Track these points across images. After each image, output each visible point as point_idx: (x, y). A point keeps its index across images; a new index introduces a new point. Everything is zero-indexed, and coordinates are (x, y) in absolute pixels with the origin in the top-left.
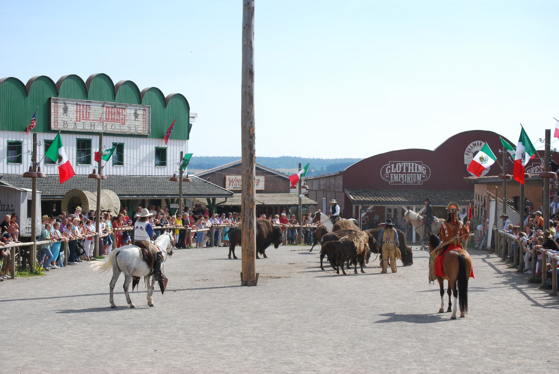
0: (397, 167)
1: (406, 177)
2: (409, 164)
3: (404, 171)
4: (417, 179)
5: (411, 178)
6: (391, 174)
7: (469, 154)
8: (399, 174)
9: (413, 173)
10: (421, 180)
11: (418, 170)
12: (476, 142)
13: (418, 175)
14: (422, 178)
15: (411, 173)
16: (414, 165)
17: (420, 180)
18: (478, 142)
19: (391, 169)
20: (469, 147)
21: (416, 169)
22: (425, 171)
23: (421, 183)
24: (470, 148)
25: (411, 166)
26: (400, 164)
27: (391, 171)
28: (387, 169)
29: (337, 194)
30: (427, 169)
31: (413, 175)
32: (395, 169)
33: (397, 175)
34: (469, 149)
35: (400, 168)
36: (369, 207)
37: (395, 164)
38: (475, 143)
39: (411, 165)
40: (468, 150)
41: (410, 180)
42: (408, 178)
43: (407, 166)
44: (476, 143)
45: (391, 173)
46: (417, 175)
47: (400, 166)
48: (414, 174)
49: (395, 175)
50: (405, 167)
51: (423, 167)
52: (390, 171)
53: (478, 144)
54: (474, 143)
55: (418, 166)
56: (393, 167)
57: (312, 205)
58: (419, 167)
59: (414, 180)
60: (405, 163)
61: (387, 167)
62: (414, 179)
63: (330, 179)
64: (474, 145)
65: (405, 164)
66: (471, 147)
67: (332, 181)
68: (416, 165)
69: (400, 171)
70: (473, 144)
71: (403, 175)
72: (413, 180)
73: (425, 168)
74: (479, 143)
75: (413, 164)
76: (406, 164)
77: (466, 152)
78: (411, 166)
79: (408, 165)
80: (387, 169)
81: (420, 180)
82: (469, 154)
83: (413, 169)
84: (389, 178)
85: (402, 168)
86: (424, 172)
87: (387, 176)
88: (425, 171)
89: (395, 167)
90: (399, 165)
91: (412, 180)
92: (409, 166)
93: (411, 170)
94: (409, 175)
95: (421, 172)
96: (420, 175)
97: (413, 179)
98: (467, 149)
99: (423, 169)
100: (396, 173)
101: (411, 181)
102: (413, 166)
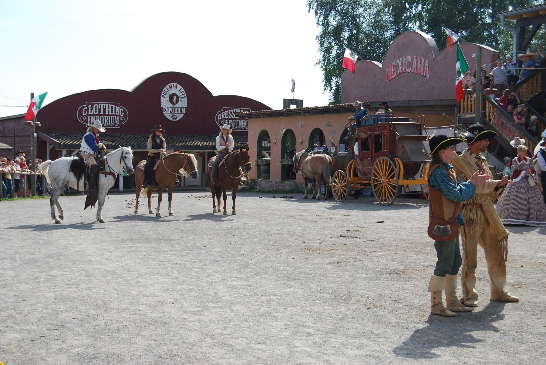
0: (94, 109)
1: (103, 119)
2: (107, 105)
3: (102, 113)
4: (114, 122)
5: (108, 121)
6: (88, 116)
7: (165, 96)
8: (97, 117)
9: (110, 115)
10: (119, 123)
11: (115, 112)
12: (172, 84)
13: (116, 117)
14: (120, 121)
15: (108, 115)
16: (112, 107)
17: (118, 123)
18: (174, 85)
19: (88, 110)
20: (165, 89)
21: (114, 111)
22: (123, 114)
23: (119, 126)
24: (166, 90)
25: (109, 108)
26: (97, 105)
27: (88, 112)
28: (84, 110)
29: (16, 140)
30: (125, 112)
31: (111, 117)
32: (92, 110)
33: (94, 117)
34: (166, 91)
35: (97, 109)
36: (73, 151)
37: (93, 105)
38: (171, 85)
39: (109, 106)
40: (165, 92)
41: (107, 123)
42: (106, 121)
43: (104, 108)
44: (172, 85)
45: (88, 115)
46: (114, 118)
47: (97, 107)
48: (112, 117)
49: (92, 117)
50: (102, 109)
51: (121, 109)
52: (87, 112)
53: (174, 87)
54: (170, 85)
55: (115, 108)
56: (90, 109)
57: (7, 151)
58: (117, 109)
59: (112, 123)
60: (103, 105)
61: (84, 109)
62: (112, 121)
63: (4, 123)
64: (170, 87)
65: (102, 105)
66: (167, 89)
67: (12, 125)
68: (114, 106)
69: (97, 113)
70: (169, 86)
71: (101, 117)
72: (111, 123)
73: (123, 110)
74: (175, 86)
75: (110, 105)
76: (103, 106)
77: (162, 94)
78: (109, 108)
79: (106, 106)
80: (84, 110)
81: (118, 123)
82: (165, 96)
83: (110, 111)
84: (86, 121)
85: (100, 110)
86: (122, 114)
87: (84, 118)
88: (123, 114)
89: (92, 108)
90: (96, 106)
91: (109, 123)
92: (107, 107)
93: (109, 112)
94: (107, 118)
95: (119, 114)
96: (118, 117)
97: (111, 122)
98: (163, 91)
99: (121, 112)
100: (93, 115)
101: (108, 124)
102: (110, 107)
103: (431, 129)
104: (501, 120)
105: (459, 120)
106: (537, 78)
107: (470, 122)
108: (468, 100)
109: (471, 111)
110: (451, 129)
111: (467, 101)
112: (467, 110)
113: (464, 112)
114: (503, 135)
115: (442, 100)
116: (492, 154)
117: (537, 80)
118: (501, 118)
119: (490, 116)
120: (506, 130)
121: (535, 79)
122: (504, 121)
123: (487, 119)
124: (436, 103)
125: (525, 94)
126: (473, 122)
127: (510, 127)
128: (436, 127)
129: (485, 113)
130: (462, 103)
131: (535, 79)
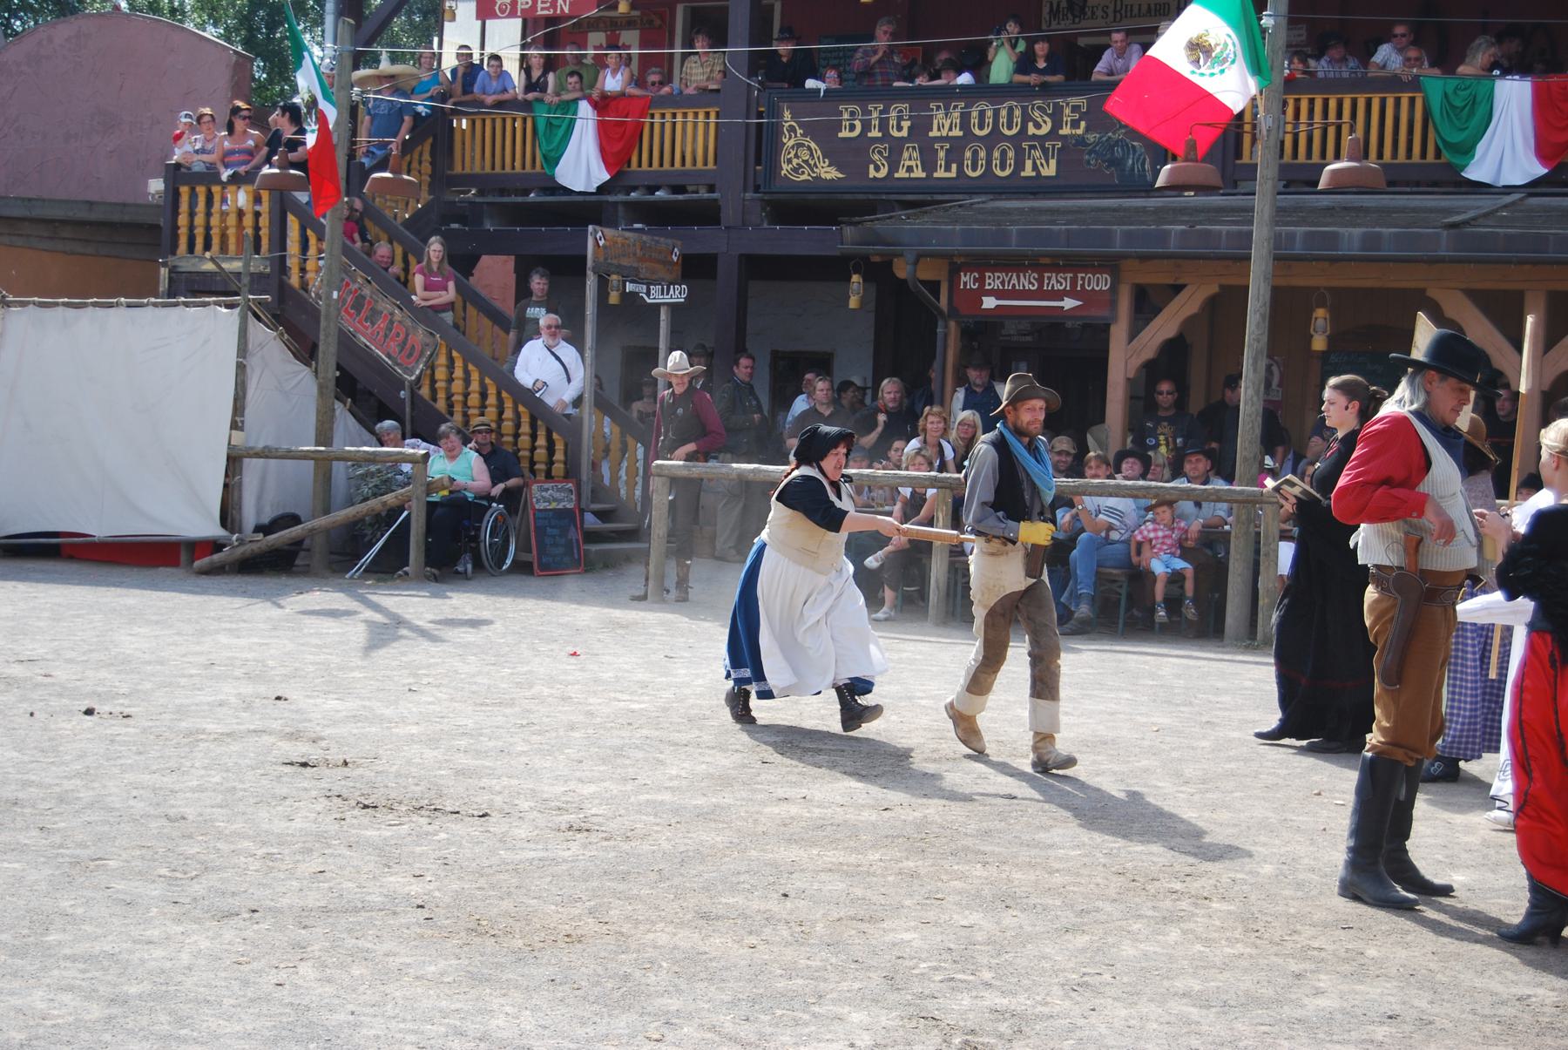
103: (186, 305)
104: (353, 287)
105: (170, 279)
106: (421, 154)
107: (220, 289)
108: (213, 210)
109: (224, 248)
110: (225, 310)
111: (208, 214)
112: (207, 247)
113: (191, 248)
114: (363, 339)
115: (91, 204)
116: (345, 404)
117: (420, 163)
118: (355, 282)
119: (303, 270)
120: (373, 324)
121: (416, 156)
122: (367, 291)
123: (294, 280)
124: (71, 214)
125: (388, 204)
126: (236, 289)
127: (392, 314)
128: (153, 300)
129: (283, 259)
130: (183, 220)
131: (416, 156)
